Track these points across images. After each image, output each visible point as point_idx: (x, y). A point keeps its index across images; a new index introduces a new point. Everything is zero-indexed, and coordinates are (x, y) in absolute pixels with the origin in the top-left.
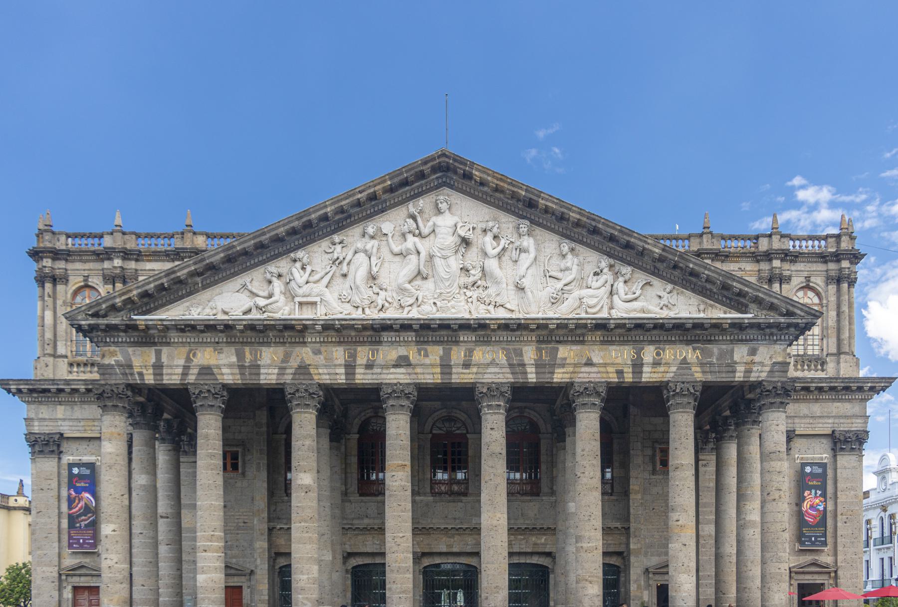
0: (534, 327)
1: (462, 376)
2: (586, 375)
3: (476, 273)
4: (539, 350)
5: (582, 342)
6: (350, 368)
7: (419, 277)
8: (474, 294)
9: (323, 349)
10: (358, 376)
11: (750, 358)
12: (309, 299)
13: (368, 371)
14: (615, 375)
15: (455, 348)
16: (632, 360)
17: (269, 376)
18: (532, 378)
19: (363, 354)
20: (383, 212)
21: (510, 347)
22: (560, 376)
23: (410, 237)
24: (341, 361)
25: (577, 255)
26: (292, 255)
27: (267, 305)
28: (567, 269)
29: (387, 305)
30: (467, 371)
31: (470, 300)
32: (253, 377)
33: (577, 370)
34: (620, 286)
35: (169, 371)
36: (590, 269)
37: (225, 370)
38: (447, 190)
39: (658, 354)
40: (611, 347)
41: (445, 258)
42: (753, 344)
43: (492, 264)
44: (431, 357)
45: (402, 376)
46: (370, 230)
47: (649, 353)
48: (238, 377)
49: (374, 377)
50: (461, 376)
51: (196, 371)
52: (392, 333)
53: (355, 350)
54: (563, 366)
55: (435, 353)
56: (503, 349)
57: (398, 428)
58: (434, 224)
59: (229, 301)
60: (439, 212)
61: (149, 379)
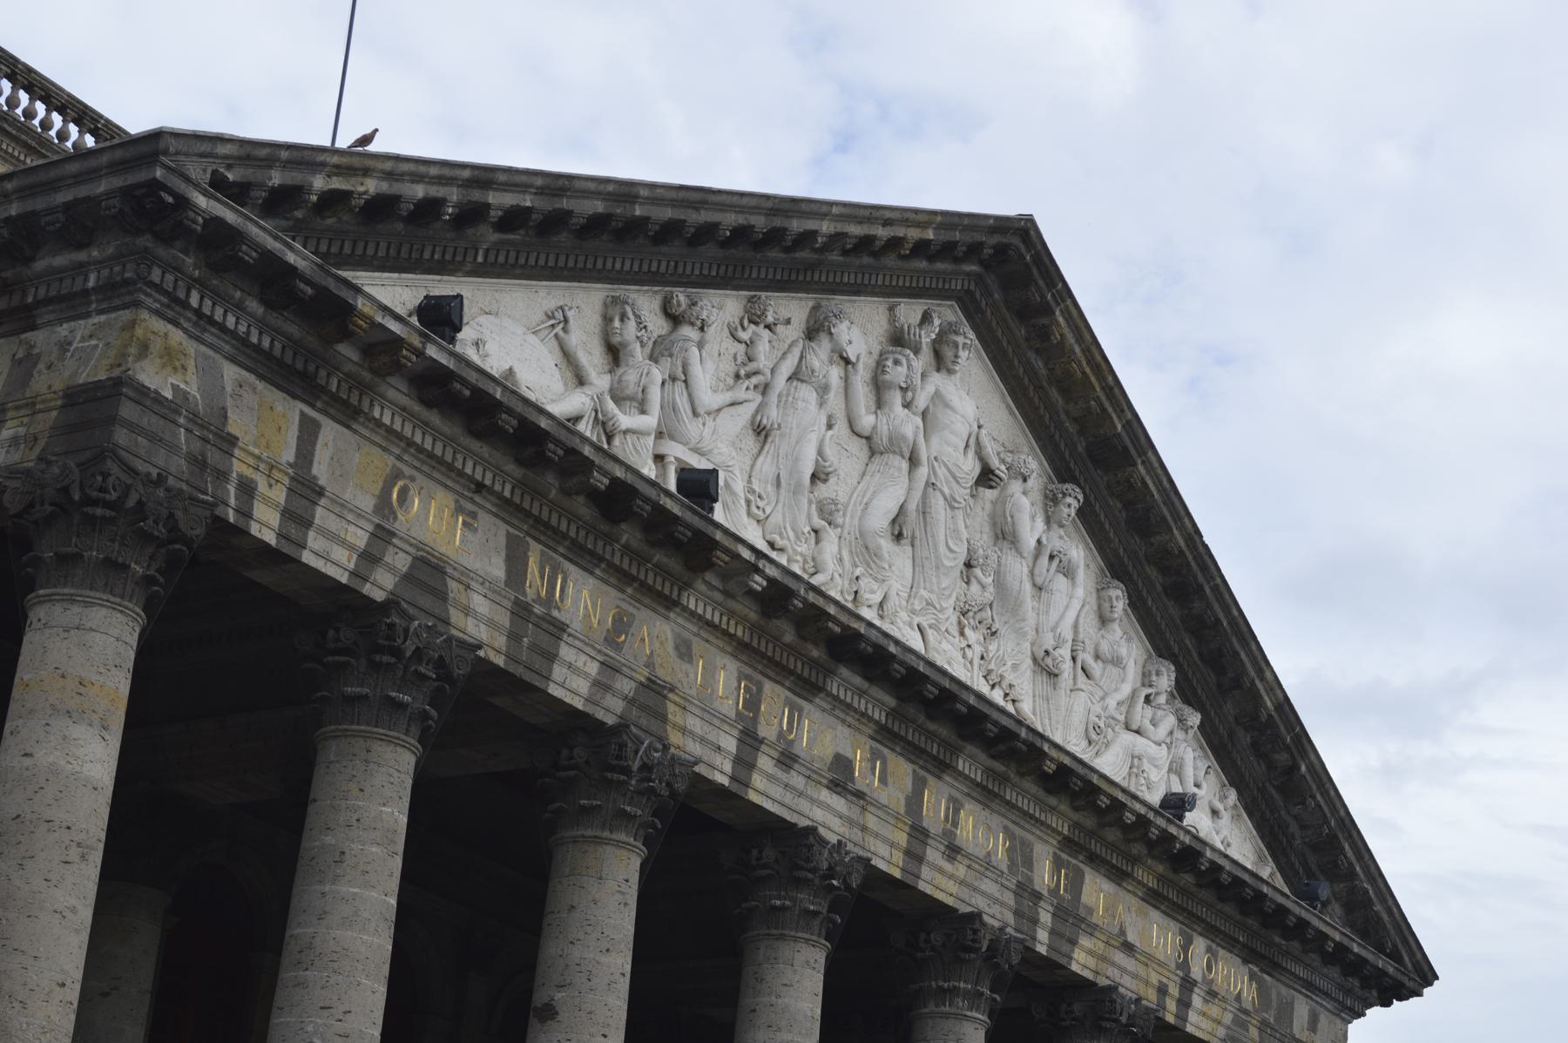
0: (1104, 802)
4: (1058, 864)
5: (1118, 876)
9: (698, 646)
10: (758, 780)
13: (780, 774)
14: (1152, 995)
15: (931, 780)
17: (572, 681)
21: (1018, 831)
22: (1081, 962)
23: (896, 398)
24: (728, 707)
26: (681, 297)
27: (626, 432)
28: (1117, 662)
31: (969, 653)
32: (538, 663)
35: (333, 524)
37: (479, 603)
40: (1155, 915)
41: (951, 503)
44: (891, 788)
45: (835, 823)
46: (843, 330)
48: (501, 641)
49: (788, 798)
51: (402, 562)
52: (857, 680)
53: (760, 690)
54: (1092, 930)
56: (1006, 830)
58: (937, 396)
60: (941, 362)
61: (266, 525)
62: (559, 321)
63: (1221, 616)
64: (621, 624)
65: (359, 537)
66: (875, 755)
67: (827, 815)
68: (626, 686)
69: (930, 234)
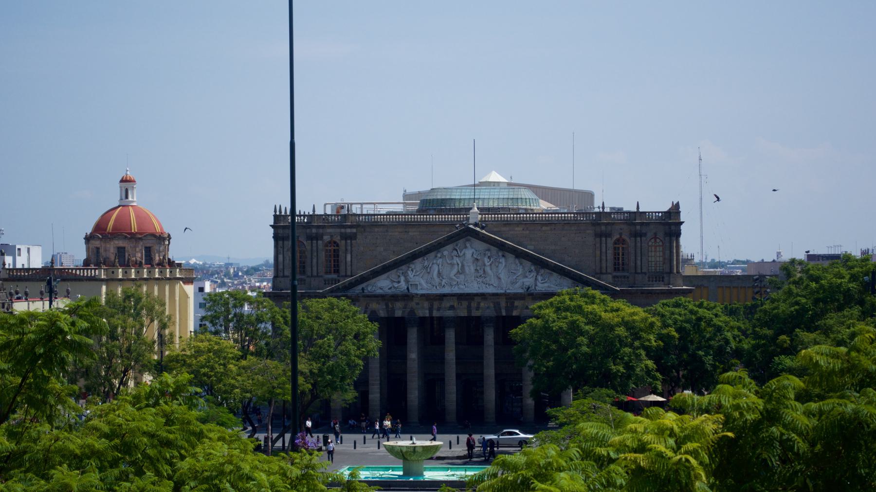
3: (481, 272)
6: (431, 310)
8: (480, 280)
17: (398, 314)
18: (504, 314)
19: (436, 304)
25: (521, 264)
34: (539, 278)
36: (526, 269)
38: (469, 237)
41: (469, 266)
43: (488, 269)
50: (475, 313)
55: (465, 304)
57: (450, 335)
60: (466, 247)
62: (388, 277)
67: (450, 313)
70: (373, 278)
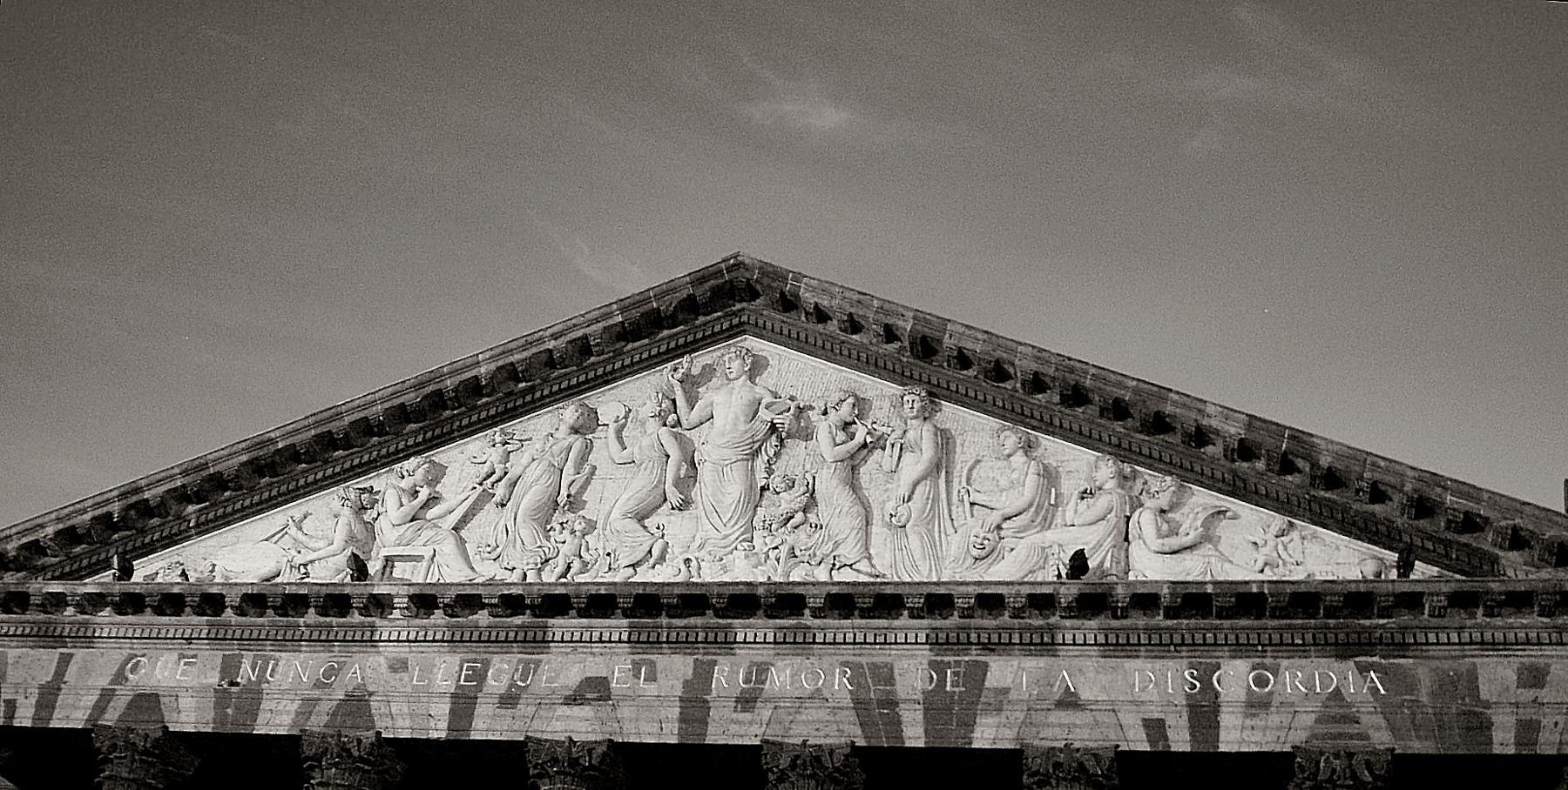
1: (734, 728)
2: (1060, 732)
6: (463, 704)
7: (666, 506)
10: (478, 723)
11: (1527, 695)
12: (407, 551)
16: (1188, 696)
18: (914, 735)
19: (502, 670)
20: (607, 383)
22: (987, 734)
24: (449, 686)
27: (312, 562)
29: (576, 566)
30: (748, 716)
31: (772, 554)
33: (1038, 717)
37: (186, 702)
39: (1261, 682)
40: (1130, 664)
42: (1533, 656)
47: (1234, 677)
53: (486, 664)
55: (676, 668)
56: (845, 664)
59: (241, 554)
63: (1120, 393)
64: (331, 672)
65: (91, 699)
66: (637, 666)
67: (579, 726)
68: (326, 707)
69: (620, 319)
70: (204, 528)
